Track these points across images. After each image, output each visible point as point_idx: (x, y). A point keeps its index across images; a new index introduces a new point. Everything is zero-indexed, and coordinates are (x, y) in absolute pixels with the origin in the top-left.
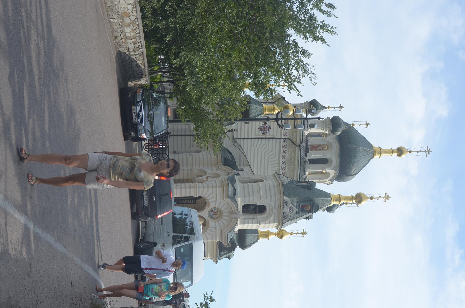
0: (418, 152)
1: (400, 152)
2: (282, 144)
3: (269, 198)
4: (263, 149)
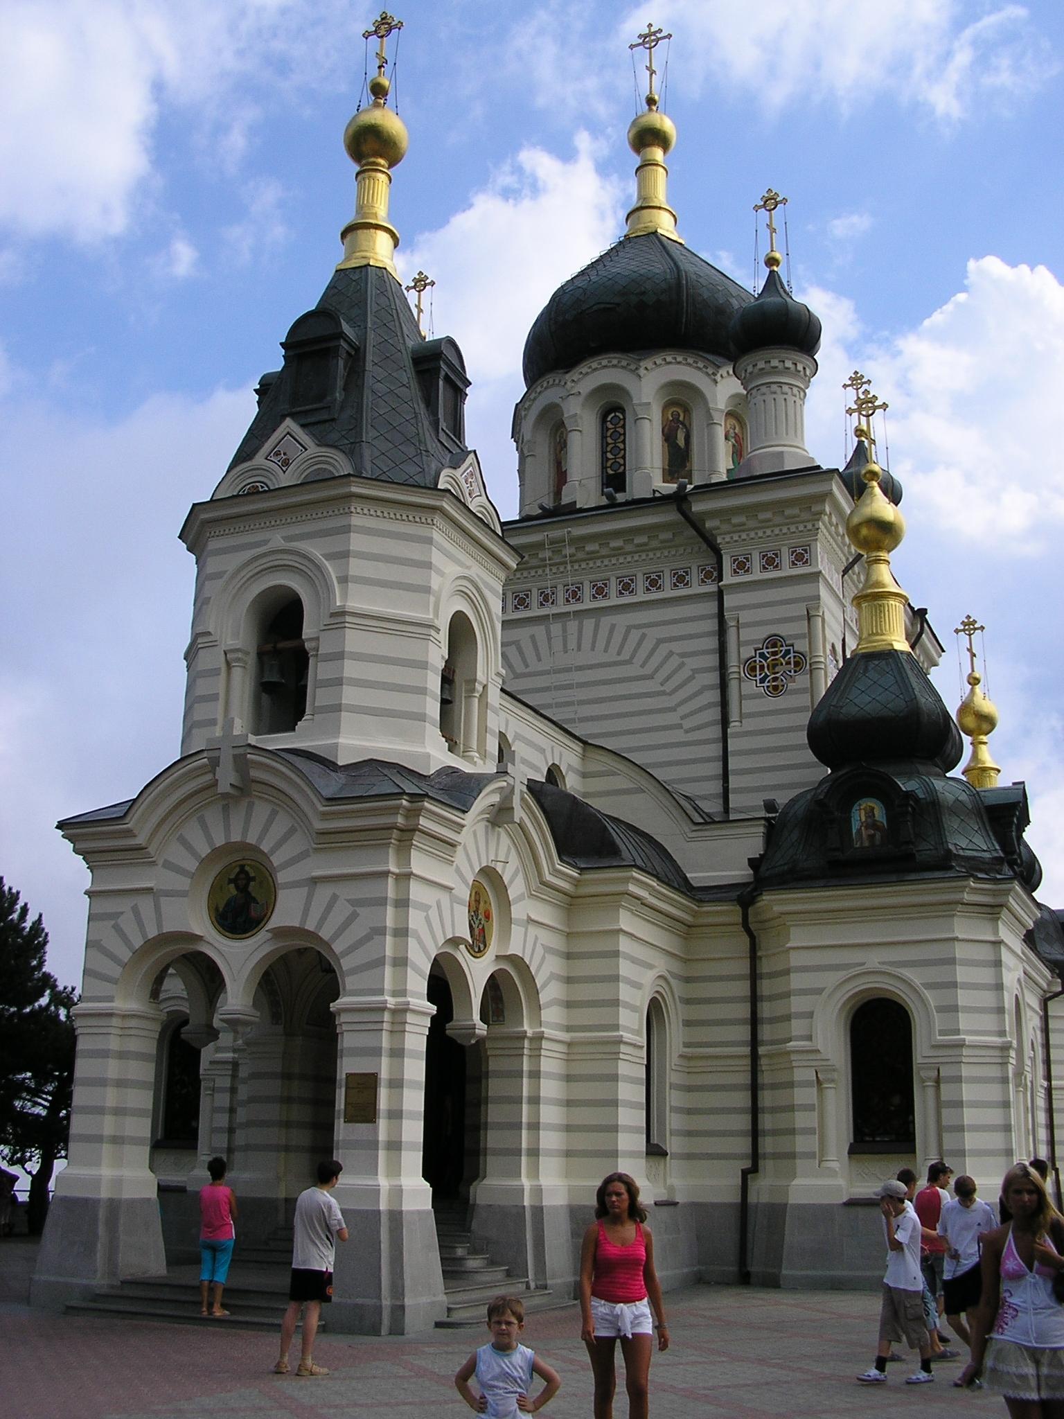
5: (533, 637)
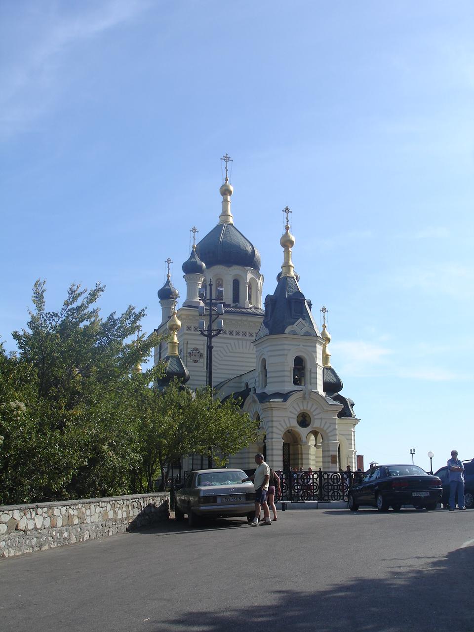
0: (227, 170)
1: (227, 192)
3: (286, 352)
4: (220, 359)
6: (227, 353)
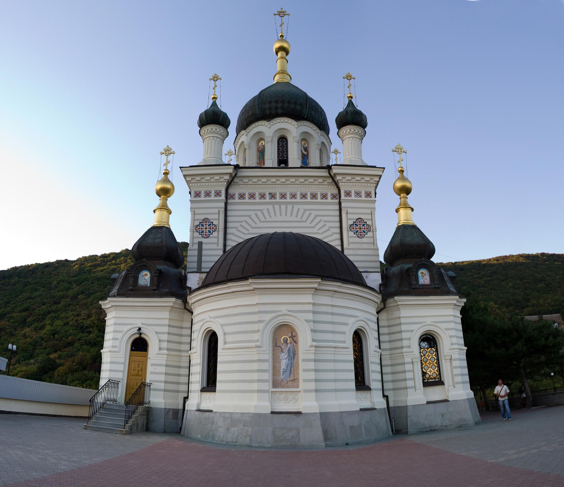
2: (237, 200)
4: (246, 232)
5: (268, 210)
6: (256, 224)
